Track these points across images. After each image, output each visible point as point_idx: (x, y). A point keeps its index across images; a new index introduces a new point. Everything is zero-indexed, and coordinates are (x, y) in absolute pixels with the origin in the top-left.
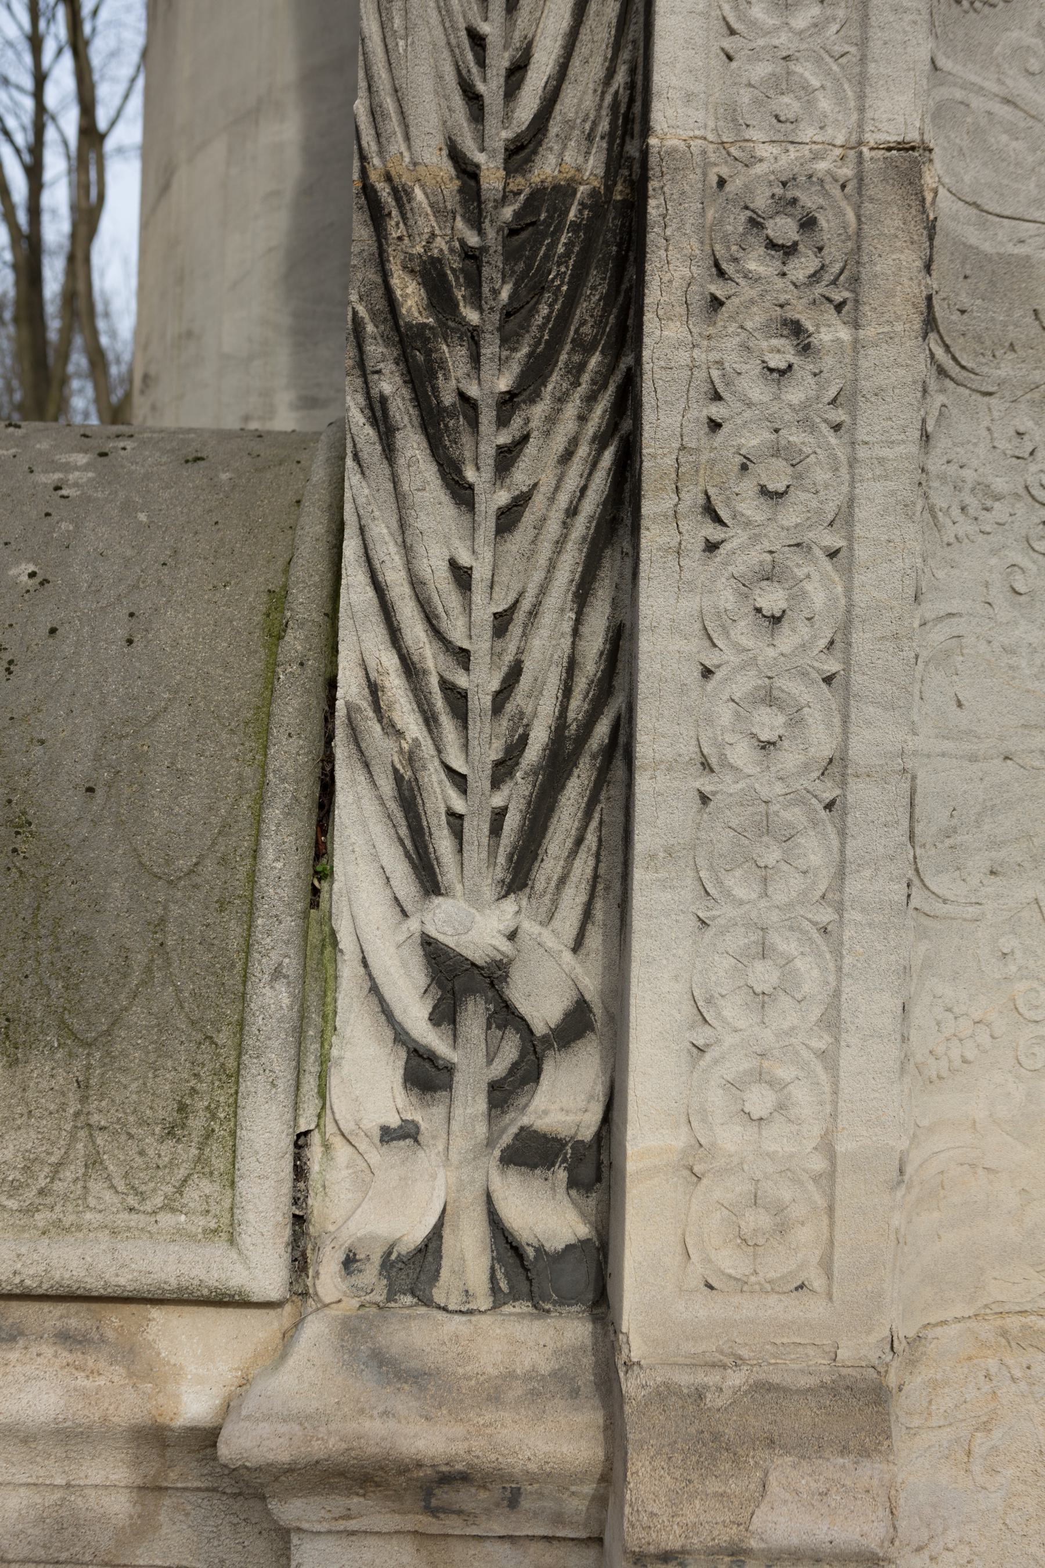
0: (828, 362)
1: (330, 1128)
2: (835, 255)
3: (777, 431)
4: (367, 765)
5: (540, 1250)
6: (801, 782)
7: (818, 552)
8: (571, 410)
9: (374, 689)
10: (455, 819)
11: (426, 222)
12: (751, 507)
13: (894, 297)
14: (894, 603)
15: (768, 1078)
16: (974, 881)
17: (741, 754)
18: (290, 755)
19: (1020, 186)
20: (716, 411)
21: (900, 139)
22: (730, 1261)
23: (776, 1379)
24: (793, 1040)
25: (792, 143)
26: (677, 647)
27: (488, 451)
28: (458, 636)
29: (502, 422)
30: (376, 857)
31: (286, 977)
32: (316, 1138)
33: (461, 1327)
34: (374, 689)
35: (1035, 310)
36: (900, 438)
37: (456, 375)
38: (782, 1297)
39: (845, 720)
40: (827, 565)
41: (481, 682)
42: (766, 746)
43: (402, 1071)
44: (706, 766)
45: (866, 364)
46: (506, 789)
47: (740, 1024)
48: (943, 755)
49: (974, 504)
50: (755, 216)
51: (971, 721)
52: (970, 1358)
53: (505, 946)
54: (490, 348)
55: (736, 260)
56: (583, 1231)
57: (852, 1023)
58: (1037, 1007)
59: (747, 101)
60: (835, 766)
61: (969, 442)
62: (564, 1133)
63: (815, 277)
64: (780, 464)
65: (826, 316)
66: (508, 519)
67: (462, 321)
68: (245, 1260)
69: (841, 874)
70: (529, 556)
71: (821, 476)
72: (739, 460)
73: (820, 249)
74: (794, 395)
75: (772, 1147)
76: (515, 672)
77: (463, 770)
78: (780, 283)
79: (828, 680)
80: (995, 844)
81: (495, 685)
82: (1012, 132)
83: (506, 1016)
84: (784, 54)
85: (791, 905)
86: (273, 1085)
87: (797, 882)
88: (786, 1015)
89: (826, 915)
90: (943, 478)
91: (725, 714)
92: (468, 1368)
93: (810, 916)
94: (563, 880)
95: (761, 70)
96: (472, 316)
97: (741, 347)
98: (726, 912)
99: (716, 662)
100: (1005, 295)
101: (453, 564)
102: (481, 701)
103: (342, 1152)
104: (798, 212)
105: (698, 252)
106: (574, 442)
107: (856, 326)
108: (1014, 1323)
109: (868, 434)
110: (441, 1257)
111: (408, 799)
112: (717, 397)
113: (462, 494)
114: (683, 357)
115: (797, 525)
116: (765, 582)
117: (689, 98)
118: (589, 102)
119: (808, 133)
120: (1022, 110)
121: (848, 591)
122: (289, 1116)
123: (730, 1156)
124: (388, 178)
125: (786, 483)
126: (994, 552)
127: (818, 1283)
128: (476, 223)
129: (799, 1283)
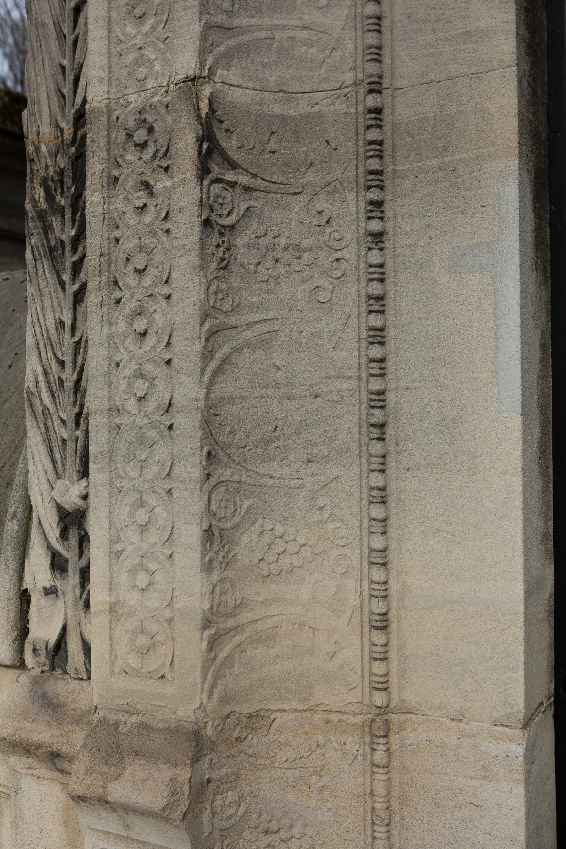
3: (140, 238)
4: (36, 418)
6: (156, 416)
7: (160, 298)
12: (131, 280)
13: (185, 159)
14: (191, 320)
15: (146, 568)
16: (295, 466)
17: (131, 405)
19: (314, 73)
20: (117, 233)
21: (185, 76)
22: (134, 661)
23: (149, 722)
24: (155, 549)
25: (143, 91)
26: (102, 353)
27: (68, 265)
31: (17, 517)
33: (76, 686)
35: (327, 141)
36: (191, 233)
38: (156, 681)
42: (141, 399)
43: (49, 562)
45: (175, 197)
47: (134, 541)
48: (263, 397)
50: (129, 132)
51: (287, 378)
52: (307, 734)
53: (80, 503)
55: (122, 156)
57: (179, 541)
58: (342, 538)
59: (125, 75)
61: (281, 223)
63: (154, 156)
65: (160, 176)
72: (126, 256)
73: (156, 142)
74: (148, 219)
75: (149, 604)
77: (65, 419)
78: (140, 163)
82: (309, 44)
84: (139, 47)
85: (153, 480)
86: (8, 566)
88: (154, 536)
92: (75, 705)
93: (161, 485)
95: (130, 58)
99: (120, 359)
100: (306, 136)
104: (147, 125)
105: (105, 156)
108: (334, 717)
109: (177, 233)
110: (67, 651)
115: (150, 285)
116: (139, 316)
119: (150, 84)
120: (315, 30)
122: (15, 581)
123: (131, 607)
125: (145, 264)
126: (303, 281)
129: (161, 675)
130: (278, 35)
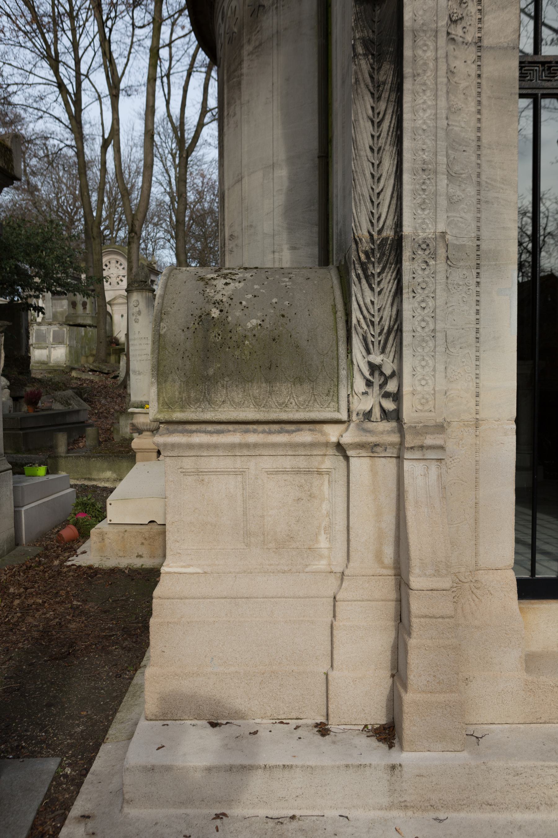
0: (431, 267)
1: (354, 393)
2: (432, 250)
5: (388, 411)
8: (389, 274)
9: (358, 322)
10: (373, 342)
11: (365, 244)
12: (420, 291)
17: (419, 329)
18: (342, 333)
20: (414, 276)
22: (419, 407)
27: (376, 282)
28: (372, 312)
29: (378, 277)
30: (359, 349)
32: (351, 395)
34: (358, 322)
37: (371, 270)
39: (435, 323)
40: (432, 299)
41: (376, 320)
42: (423, 328)
44: (414, 331)
46: (381, 337)
49: (456, 287)
53: (381, 362)
54: (376, 265)
56: (395, 407)
60: (434, 331)
62: (392, 392)
63: (429, 254)
64: (424, 284)
66: (380, 293)
67: (371, 260)
68: (341, 414)
69: (435, 347)
70: (384, 299)
71: (431, 285)
74: (426, 273)
76: (382, 318)
79: (432, 317)
80: (461, 343)
81: (378, 320)
82: (462, 223)
83: (382, 374)
87: (428, 349)
88: (427, 369)
89: (433, 354)
90: (451, 283)
91: (417, 323)
94: (390, 351)
95: (420, 221)
96: (373, 259)
97: (418, 265)
98: (417, 354)
101: (371, 301)
102: (376, 323)
103: (355, 397)
106: (390, 280)
107: (436, 261)
108: (466, 423)
111: (365, 339)
112: (414, 273)
113: (372, 289)
114: (409, 267)
117: (409, 226)
118: (391, 223)
119: (428, 231)
121: (435, 303)
124: (358, 237)
127: (433, 410)
128: (373, 244)
130: (455, 219)
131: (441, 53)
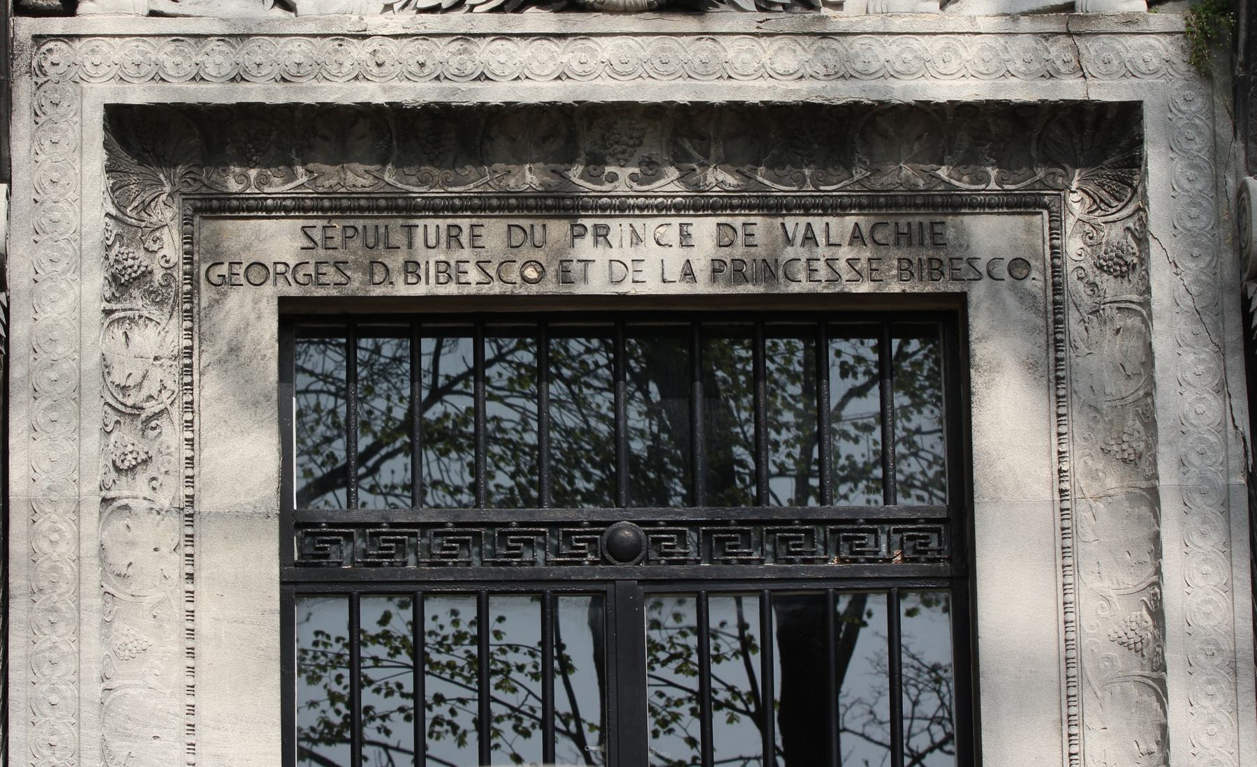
131: (89, 547)
